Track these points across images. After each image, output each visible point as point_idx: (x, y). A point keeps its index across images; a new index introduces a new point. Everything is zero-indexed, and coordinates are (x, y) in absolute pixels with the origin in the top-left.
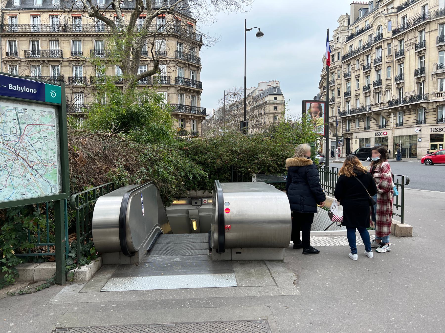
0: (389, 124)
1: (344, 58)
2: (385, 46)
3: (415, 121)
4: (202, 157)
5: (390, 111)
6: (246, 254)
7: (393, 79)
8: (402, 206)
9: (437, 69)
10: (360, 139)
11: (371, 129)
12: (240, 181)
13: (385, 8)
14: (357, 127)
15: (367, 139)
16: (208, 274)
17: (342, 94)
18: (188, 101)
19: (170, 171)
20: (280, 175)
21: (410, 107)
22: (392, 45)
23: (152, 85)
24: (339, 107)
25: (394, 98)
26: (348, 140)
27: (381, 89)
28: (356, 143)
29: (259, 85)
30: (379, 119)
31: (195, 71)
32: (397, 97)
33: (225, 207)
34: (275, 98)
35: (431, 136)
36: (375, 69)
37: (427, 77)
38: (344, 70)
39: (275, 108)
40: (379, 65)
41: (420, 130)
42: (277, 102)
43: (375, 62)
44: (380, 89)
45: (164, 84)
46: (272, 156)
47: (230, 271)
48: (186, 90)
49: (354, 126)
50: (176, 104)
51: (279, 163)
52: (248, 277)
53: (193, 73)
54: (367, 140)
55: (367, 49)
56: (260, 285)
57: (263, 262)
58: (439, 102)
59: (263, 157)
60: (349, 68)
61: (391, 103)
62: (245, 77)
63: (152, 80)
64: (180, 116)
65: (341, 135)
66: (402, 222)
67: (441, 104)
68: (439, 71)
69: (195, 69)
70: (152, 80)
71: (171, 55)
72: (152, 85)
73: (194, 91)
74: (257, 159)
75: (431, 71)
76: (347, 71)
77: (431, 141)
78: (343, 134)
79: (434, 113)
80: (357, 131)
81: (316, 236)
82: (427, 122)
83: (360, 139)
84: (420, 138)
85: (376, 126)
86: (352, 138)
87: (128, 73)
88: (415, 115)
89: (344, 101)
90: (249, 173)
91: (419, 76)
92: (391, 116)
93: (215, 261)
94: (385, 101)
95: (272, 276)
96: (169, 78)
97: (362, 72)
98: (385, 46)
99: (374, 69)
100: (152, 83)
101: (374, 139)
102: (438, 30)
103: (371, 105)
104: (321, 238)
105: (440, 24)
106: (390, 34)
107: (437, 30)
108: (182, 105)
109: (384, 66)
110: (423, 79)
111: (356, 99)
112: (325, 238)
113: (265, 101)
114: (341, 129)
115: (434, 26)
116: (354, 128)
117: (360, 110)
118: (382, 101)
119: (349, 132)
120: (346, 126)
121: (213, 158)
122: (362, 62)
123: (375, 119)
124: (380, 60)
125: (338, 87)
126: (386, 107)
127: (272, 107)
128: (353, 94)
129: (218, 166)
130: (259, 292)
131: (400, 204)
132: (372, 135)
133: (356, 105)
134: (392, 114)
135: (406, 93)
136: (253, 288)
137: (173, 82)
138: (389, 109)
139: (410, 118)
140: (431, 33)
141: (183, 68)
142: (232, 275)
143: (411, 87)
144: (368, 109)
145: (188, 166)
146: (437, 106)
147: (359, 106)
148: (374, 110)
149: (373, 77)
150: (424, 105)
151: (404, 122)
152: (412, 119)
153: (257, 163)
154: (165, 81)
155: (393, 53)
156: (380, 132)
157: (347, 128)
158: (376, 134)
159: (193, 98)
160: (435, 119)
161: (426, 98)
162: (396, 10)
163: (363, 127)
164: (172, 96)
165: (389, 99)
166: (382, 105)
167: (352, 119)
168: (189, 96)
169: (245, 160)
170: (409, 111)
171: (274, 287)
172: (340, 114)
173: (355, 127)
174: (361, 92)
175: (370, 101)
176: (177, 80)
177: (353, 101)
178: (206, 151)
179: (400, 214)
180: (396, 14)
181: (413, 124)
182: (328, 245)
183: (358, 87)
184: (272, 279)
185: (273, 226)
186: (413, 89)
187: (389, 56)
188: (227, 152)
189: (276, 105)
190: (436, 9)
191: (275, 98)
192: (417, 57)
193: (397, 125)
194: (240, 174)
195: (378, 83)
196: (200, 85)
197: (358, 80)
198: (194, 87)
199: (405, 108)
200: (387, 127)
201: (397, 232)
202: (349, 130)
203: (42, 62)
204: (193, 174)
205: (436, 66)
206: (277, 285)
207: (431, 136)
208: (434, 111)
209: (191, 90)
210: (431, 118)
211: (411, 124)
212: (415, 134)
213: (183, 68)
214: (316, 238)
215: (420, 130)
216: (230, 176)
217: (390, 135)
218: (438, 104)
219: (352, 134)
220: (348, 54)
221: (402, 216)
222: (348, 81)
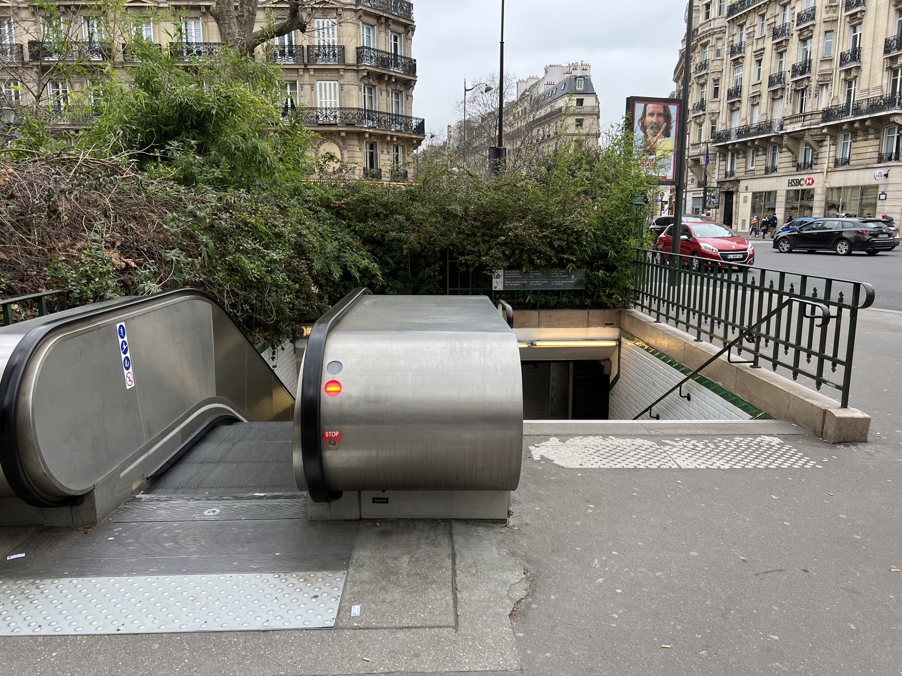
0: (819, 161)
1: (732, 9)
3: (876, 155)
4: (374, 227)
5: (825, 131)
6: (402, 505)
7: (837, 60)
8: (848, 364)
10: (754, 193)
11: (781, 172)
12: (415, 292)
14: (750, 168)
15: (770, 192)
16: (272, 570)
17: (723, 94)
18: (384, 102)
19: (273, 261)
20: (556, 272)
23: (306, 65)
24: (714, 122)
26: (729, 195)
27: (809, 81)
28: (745, 201)
29: (546, 72)
30: (798, 149)
31: (400, 34)
32: (843, 101)
33: (327, 377)
36: (799, 35)
38: (731, 39)
39: (580, 123)
40: (808, 27)
41: (886, 176)
44: (805, 83)
45: (332, 63)
46: (542, 226)
47: (337, 561)
48: (380, 77)
49: (744, 165)
50: (359, 109)
51: (556, 244)
52: (383, 588)
53: (396, 39)
54: (770, 195)
56: (405, 622)
57: (445, 525)
59: (517, 228)
60: (741, 34)
61: (827, 114)
62: (502, 43)
63: (306, 54)
64: (367, 136)
65: (715, 185)
66: (844, 405)
69: (401, 30)
70: (306, 54)
72: (306, 65)
74: (503, 232)
76: (737, 41)
78: (718, 182)
80: (749, 175)
81: (616, 436)
83: (754, 193)
84: (883, 193)
85: (791, 164)
86: (737, 191)
87: (230, 28)
88: (877, 142)
89: (725, 109)
90: (483, 266)
92: (825, 143)
93: (313, 522)
94: (815, 108)
95: (454, 582)
96: (343, 49)
97: (769, 44)
100: (306, 61)
101: (784, 193)
103: (785, 119)
104: (629, 441)
108: (372, 111)
111: (753, 105)
112: (639, 441)
114: (716, 171)
116: (744, 170)
117: (760, 129)
118: (808, 109)
119: (732, 178)
120: (726, 165)
121: (401, 229)
122: (772, 20)
123: (789, 150)
125: (715, 76)
126: (815, 123)
127: (571, 121)
128: (745, 94)
129: (411, 250)
130: (393, 653)
131: (842, 355)
132: (780, 185)
133: (752, 119)
134: (828, 138)
135: (861, 91)
136: (379, 635)
137: (351, 58)
138: (823, 128)
139: (867, 148)
141: (373, 26)
142: (339, 578)
144: (776, 128)
145: (331, 247)
148: (789, 129)
149: (794, 55)
151: (853, 157)
152: (871, 150)
153: (505, 244)
154: (334, 55)
156: (799, 178)
157: (729, 170)
158: (790, 183)
159: (397, 95)
163: (764, 167)
164: (349, 90)
165: (824, 102)
167: (741, 150)
168: (387, 92)
169: (474, 234)
171: (445, 632)
172: (717, 137)
173: (746, 168)
174: (765, 89)
175: (783, 108)
176: (359, 52)
178: (389, 210)
179: (841, 383)
181: (871, 161)
182: (642, 466)
183: (759, 78)
184: (449, 598)
185: (469, 435)
186: (879, 84)
188: (432, 214)
189: (580, 117)
191: (580, 102)
193: (836, 163)
194: (463, 269)
195: (804, 68)
196: (411, 67)
197: (759, 62)
198: (397, 71)
199: (856, 125)
200: (814, 167)
201: (830, 429)
202: (732, 174)
203: (63, 9)
204: (344, 268)
206: (456, 627)
209: (390, 77)
212: (874, 182)
213: (373, 26)
214: (617, 441)
215: (886, 176)
216: (442, 271)
217: (821, 185)
219: (738, 181)
221: (845, 389)
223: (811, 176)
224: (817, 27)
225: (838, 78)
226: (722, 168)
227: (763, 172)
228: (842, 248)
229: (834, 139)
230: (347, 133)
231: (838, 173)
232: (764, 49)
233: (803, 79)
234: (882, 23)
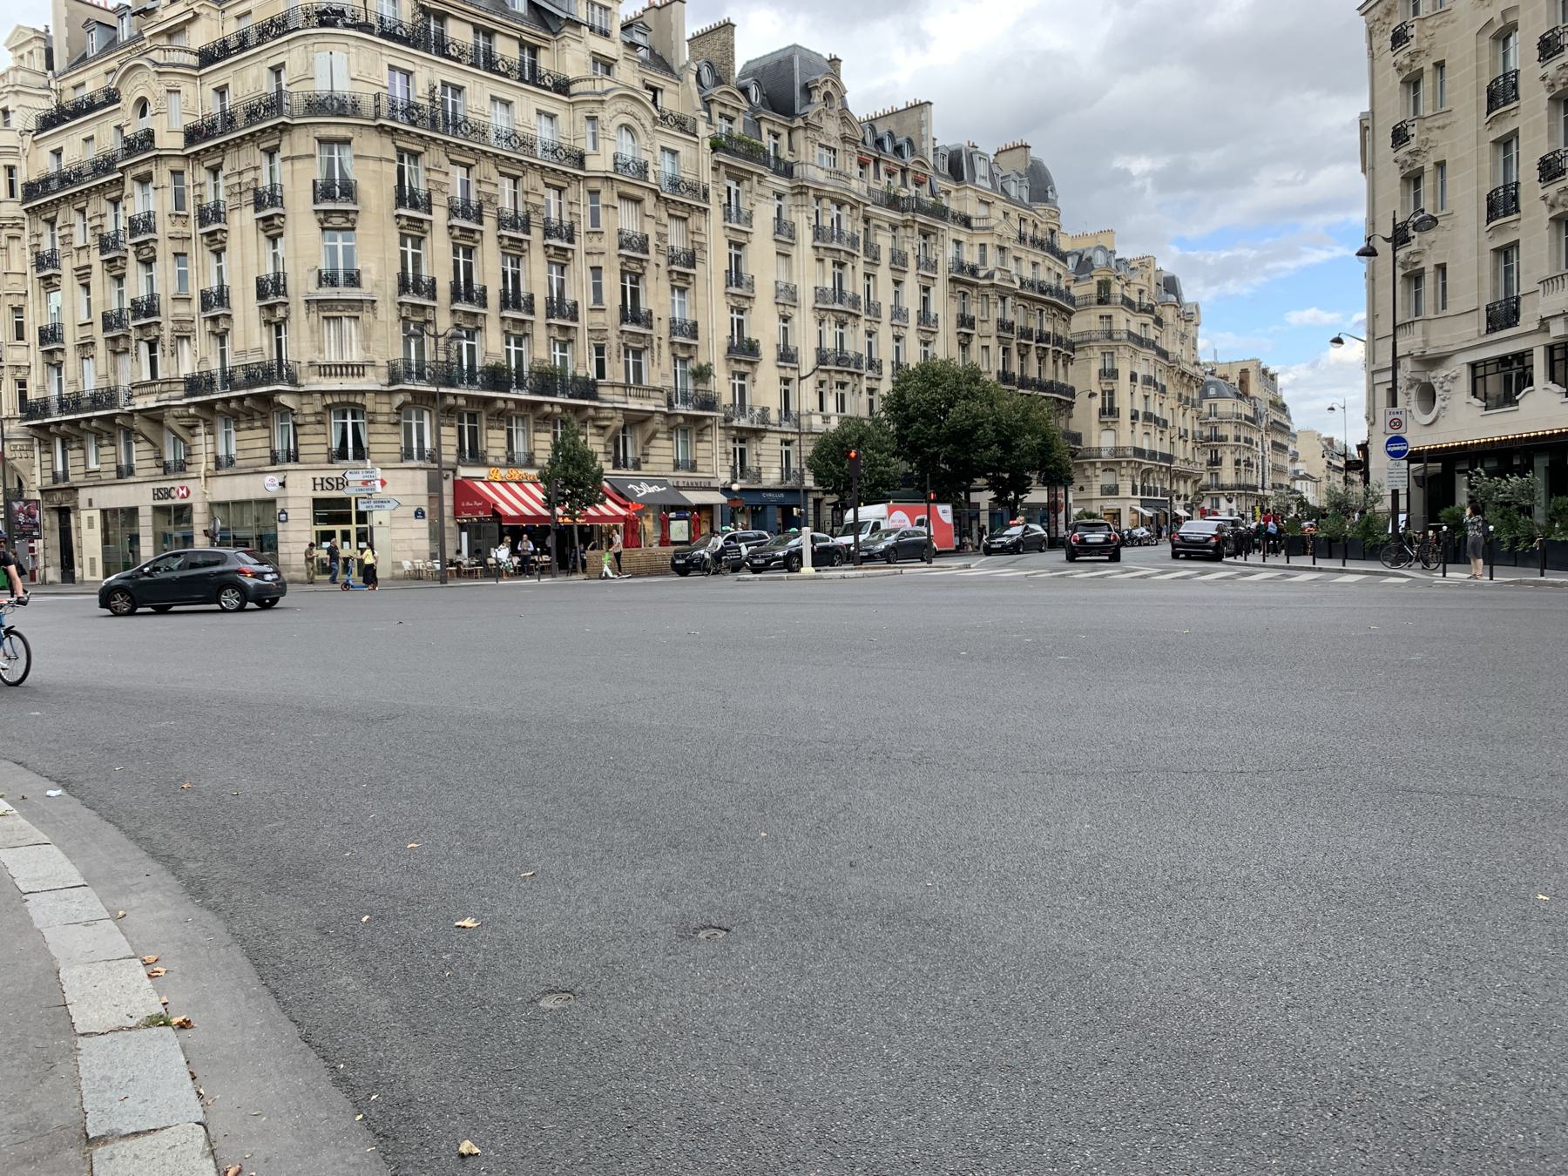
0: (194, 459)
2: (162, 175)
3: (267, 452)
5: (192, 411)
7: (197, 302)
9: (320, 285)
10: (104, 512)
11: (140, 475)
13: (163, 41)
14: (93, 466)
17: (32, 335)
21: (247, 403)
25: (203, 369)
26: (64, 513)
28: (91, 526)
30: (161, 438)
35: (317, 503)
36: (137, 253)
37: (292, 306)
38: (34, 241)
40: (146, 242)
41: (283, 484)
43: (134, 227)
44: (154, 331)
49: (81, 462)
54: (132, 513)
55: (105, 180)
58: (331, 393)
61: (194, 385)
65: (38, 496)
67: (336, 400)
68: (327, 293)
75: (302, 288)
76: (46, 246)
77: (318, 519)
78: (42, 492)
79: (320, 428)
80: (93, 479)
82: (301, 458)
83: (104, 512)
84: (283, 512)
86: (76, 507)
88: (265, 433)
89: (40, 362)
91: (271, 300)
92: (198, 430)
94: (173, 374)
97: (96, 259)
98: (162, 175)
99: (131, 256)
101: (149, 511)
102: (317, 160)
103: (135, 386)
105: (321, 141)
106: (178, 141)
107: (313, 156)
109: (164, 250)
110: (280, 312)
114: (37, 470)
115: (301, 142)
116: (82, 470)
117: (96, 400)
119: (62, 485)
120: (53, 461)
122: (96, 222)
123: (147, 440)
126: (176, 397)
128: (70, 338)
132: (139, 496)
135: (237, 353)
138: (188, 405)
140: (298, 165)
143: (250, 339)
144: (122, 399)
146: (328, 407)
147: (90, 385)
148: (140, 403)
149: (136, 285)
150: (285, 400)
152: (260, 443)
155: (191, 209)
156: (168, 485)
157: (60, 468)
158: (158, 494)
160: (324, 449)
161: (293, 380)
162: (194, 60)
163: (113, 467)
165: (187, 368)
166: (166, 387)
167: (73, 435)
170: (250, 415)
172: (29, 409)
173: (86, 465)
174: (99, 335)
175: (133, 369)
177: (71, 359)
180: (195, 73)
181: (262, 461)
183: (89, 315)
186: (257, 344)
187: (179, 214)
190: (307, 87)
192: (262, 235)
193: (217, 461)
195: (147, 308)
197: (86, 286)
199: (233, 405)
202: (66, 478)
205: (314, 277)
207: (317, 503)
208: (319, 423)
210: (317, 443)
211: (258, 461)
212: (268, 496)
215: (283, 484)
217: (200, 498)
218: (329, 401)
219: (76, 489)
220: (45, 181)
222: (49, 283)
223: (185, 483)
224: (160, 243)
225: (202, 328)
226: (47, 465)
227: (114, 475)
228: (230, 599)
229: (210, 425)
231: (220, 480)
232: (89, 267)
233: (149, 325)
234: (252, 258)
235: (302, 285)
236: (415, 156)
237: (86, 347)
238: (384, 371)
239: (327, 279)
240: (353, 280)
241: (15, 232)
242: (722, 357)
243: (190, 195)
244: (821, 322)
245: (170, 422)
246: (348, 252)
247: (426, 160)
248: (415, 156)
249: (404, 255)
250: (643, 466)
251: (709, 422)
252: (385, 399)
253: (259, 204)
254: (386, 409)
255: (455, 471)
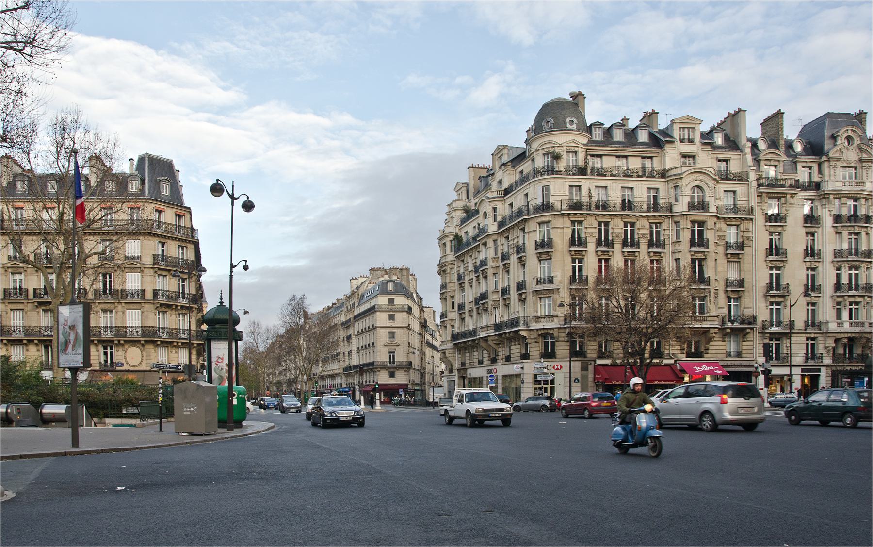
2: (490, 243)
22: (499, 243)
34: (391, 301)
39: (392, 317)
42: (393, 308)
48: (169, 306)
58: (541, 329)
68: (540, 287)
71: (148, 260)
73: (182, 307)
96: (143, 291)
98: (490, 243)
105: (539, 224)
109: (490, 272)
113: (372, 305)
124: (484, 263)
137: (149, 296)
139: (516, 350)
176: (155, 293)
191: (391, 301)
209: (177, 306)
230: (145, 341)
235: (531, 285)
236: (580, 223)
237: (471, 311)
238: (563, 319)
239: (539, 282)
240: (551, 280)
241: (452, 266)
242: (761, 294)
243: (499, 248)
244: (838, 269)
245: (490, 342)
246: (549, 268)
247: (585, 224)
248: (580, 223)
249: (574, 267)
250: (706, 356)
251: (748, 330)
252: (562, 331)
253: (518, 252)
254: (563, 335)
255: (595, 362)
